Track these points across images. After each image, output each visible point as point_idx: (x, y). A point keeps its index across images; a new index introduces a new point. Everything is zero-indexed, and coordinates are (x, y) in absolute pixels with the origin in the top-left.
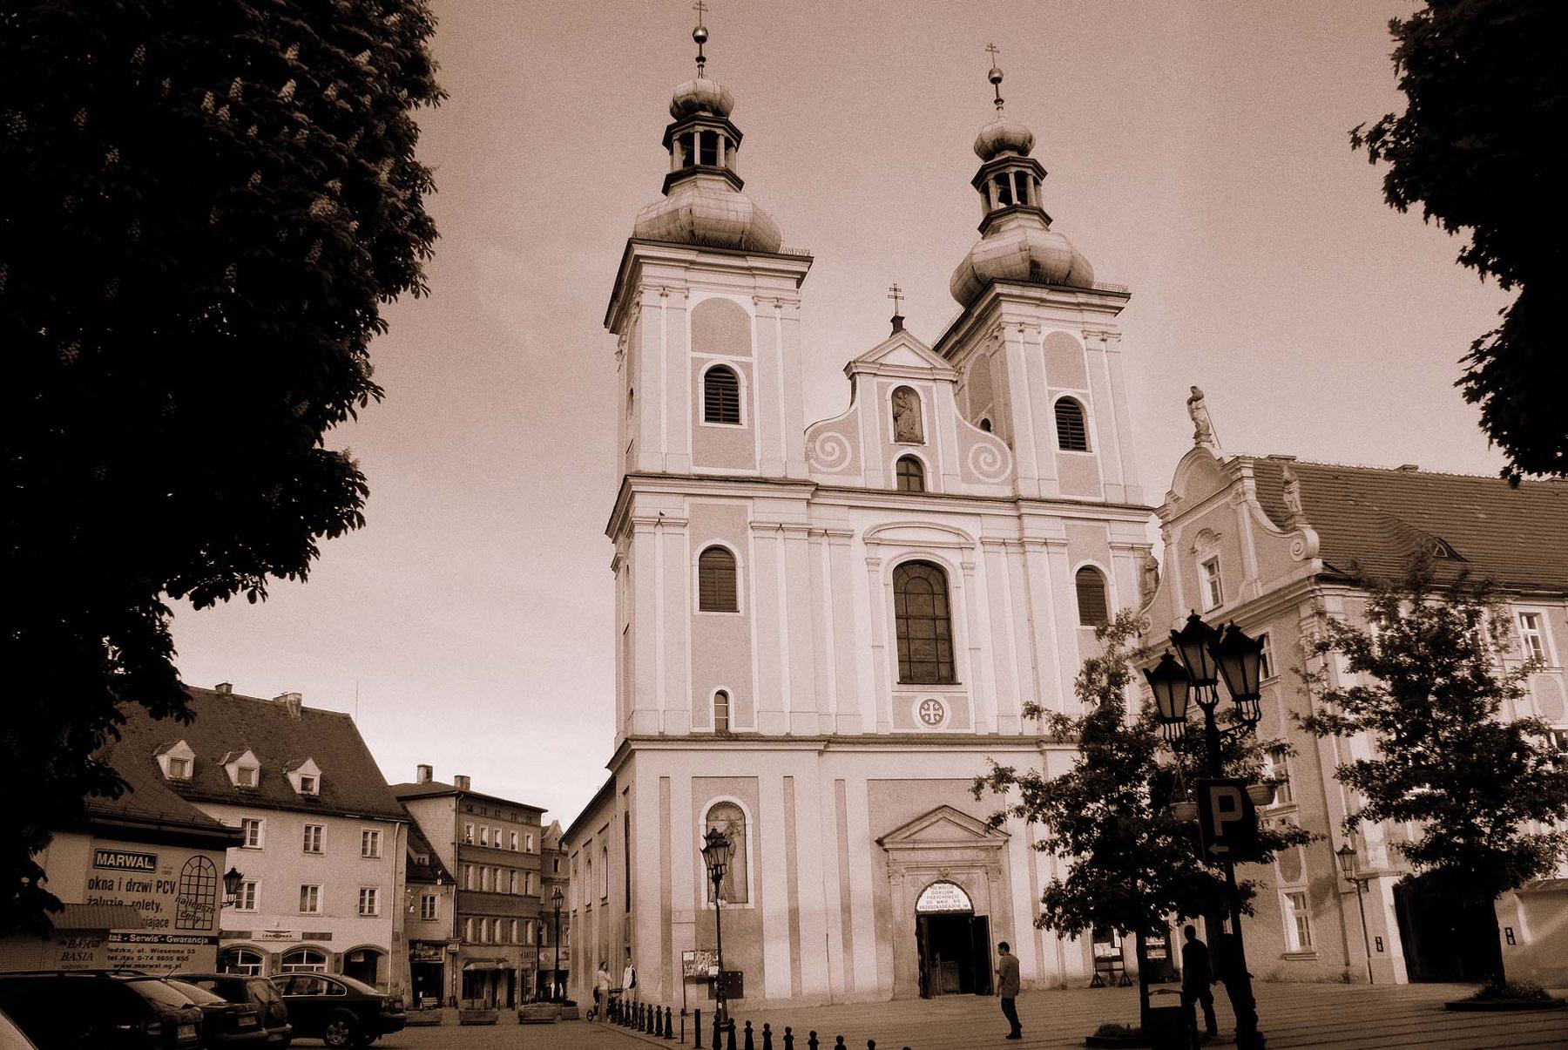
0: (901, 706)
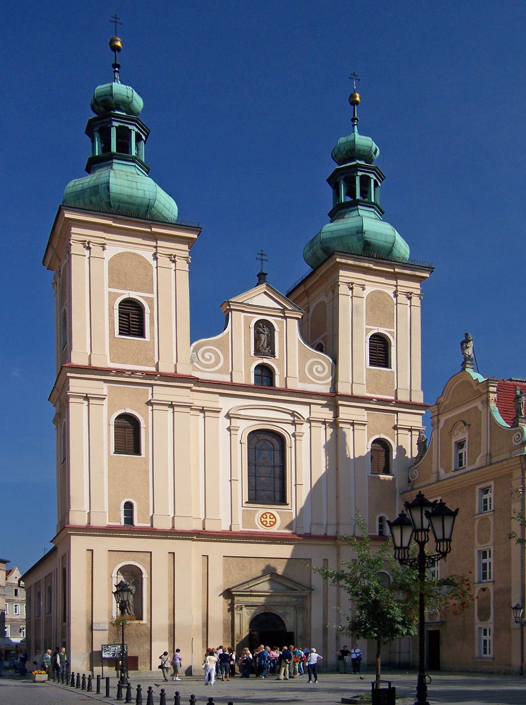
0: (248, 517)
